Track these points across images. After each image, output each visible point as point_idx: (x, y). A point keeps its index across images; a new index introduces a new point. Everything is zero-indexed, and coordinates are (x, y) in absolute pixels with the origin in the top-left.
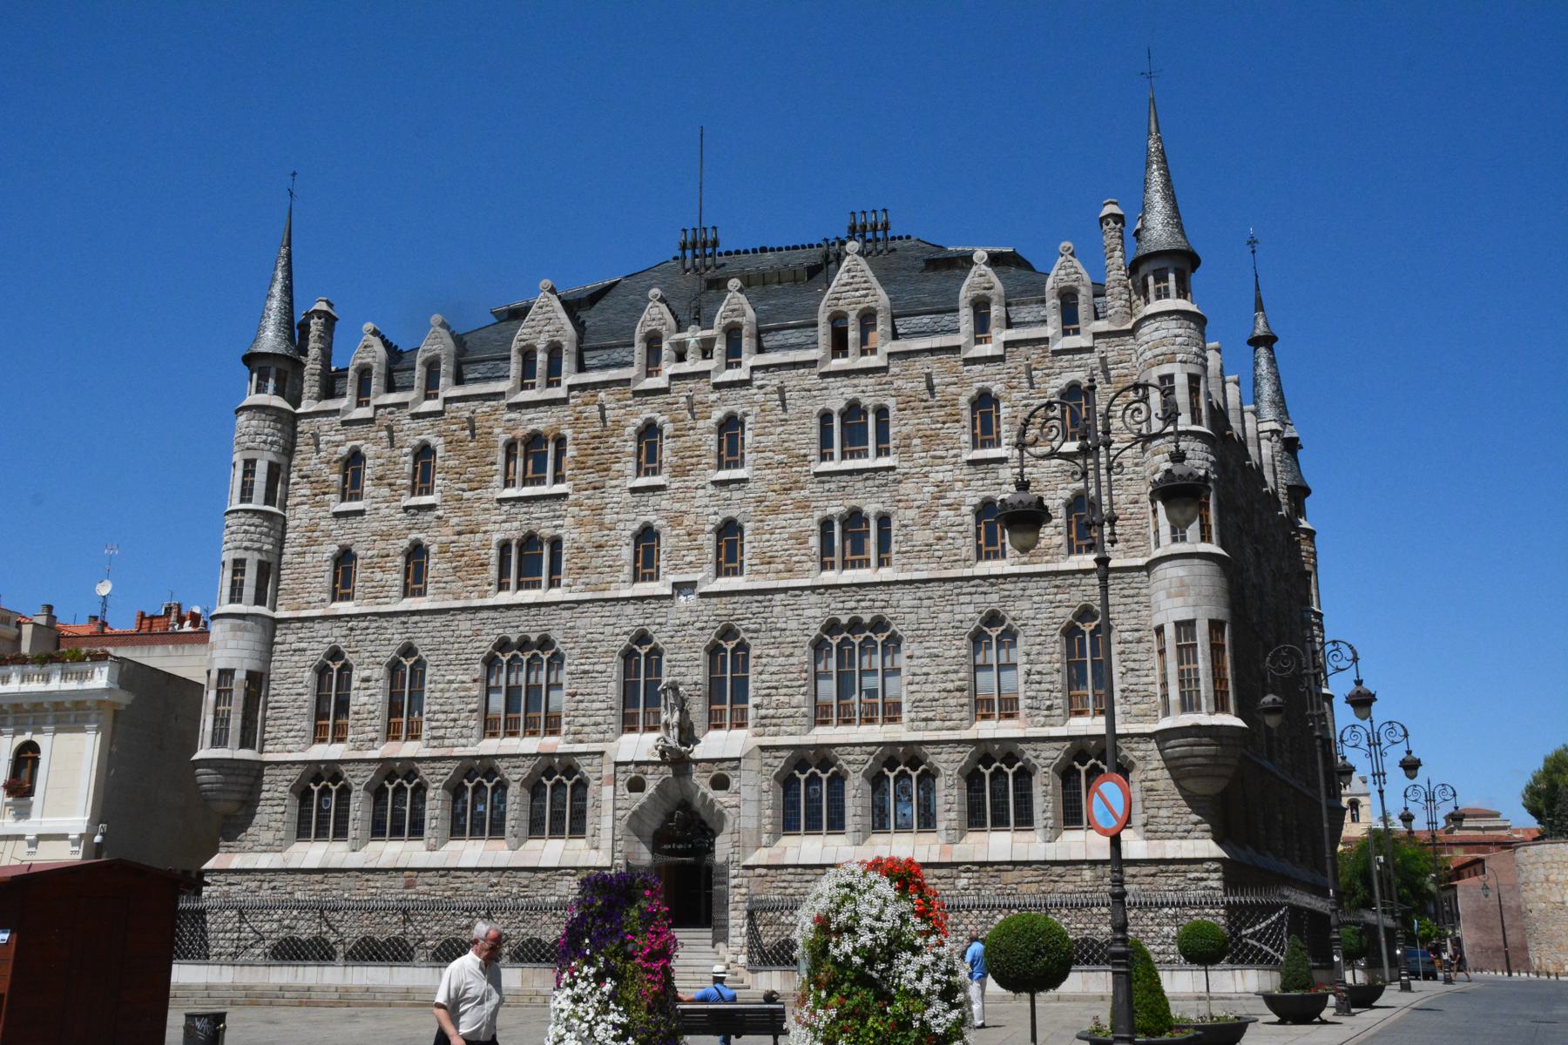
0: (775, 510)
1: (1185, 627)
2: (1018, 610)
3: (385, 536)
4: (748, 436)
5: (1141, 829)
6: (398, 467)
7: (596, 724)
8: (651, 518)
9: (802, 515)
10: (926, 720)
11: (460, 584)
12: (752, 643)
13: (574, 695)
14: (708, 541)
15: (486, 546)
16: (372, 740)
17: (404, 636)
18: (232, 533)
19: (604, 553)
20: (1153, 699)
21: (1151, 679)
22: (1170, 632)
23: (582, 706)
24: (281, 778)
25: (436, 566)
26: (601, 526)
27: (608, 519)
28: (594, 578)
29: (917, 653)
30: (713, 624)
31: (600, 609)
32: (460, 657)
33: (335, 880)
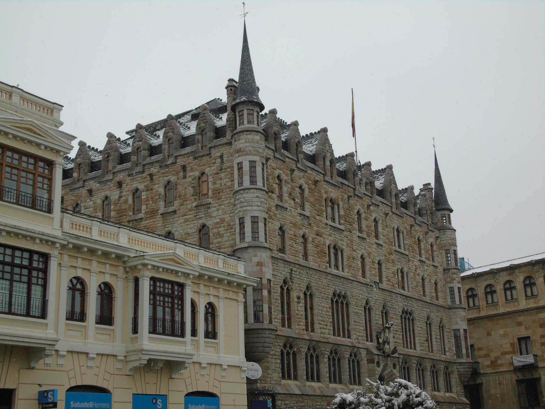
0: (388, 260)
1: (465, 331)
2: (433, 316)
3: (295, 225)
4: (380, 229)
5: (456, 394)
6: (295, 192)
7: (362, 336)
8: (363, 251)
9: (393, 265)
10: (422, 350)
11: (320, 260)
12: (391, 312)
13: (355, 322)
14: (376, 266)
15: (324, 244)
16: (303, 330)
17: (308, 279)
18: (262, 202)
19: (354, 261)
20: (452, 352)
21: (452, 345)
22: (462, 332)
23: (358, 327)
24: (277, 344)
25: (310, 246)
26: (354, 251)
27: (355, 247)
28: (353, 272)
29: (419, 326)
30: (382, 302)
31: (357, 286)
32: (326, 296)
33: (306, 401)
